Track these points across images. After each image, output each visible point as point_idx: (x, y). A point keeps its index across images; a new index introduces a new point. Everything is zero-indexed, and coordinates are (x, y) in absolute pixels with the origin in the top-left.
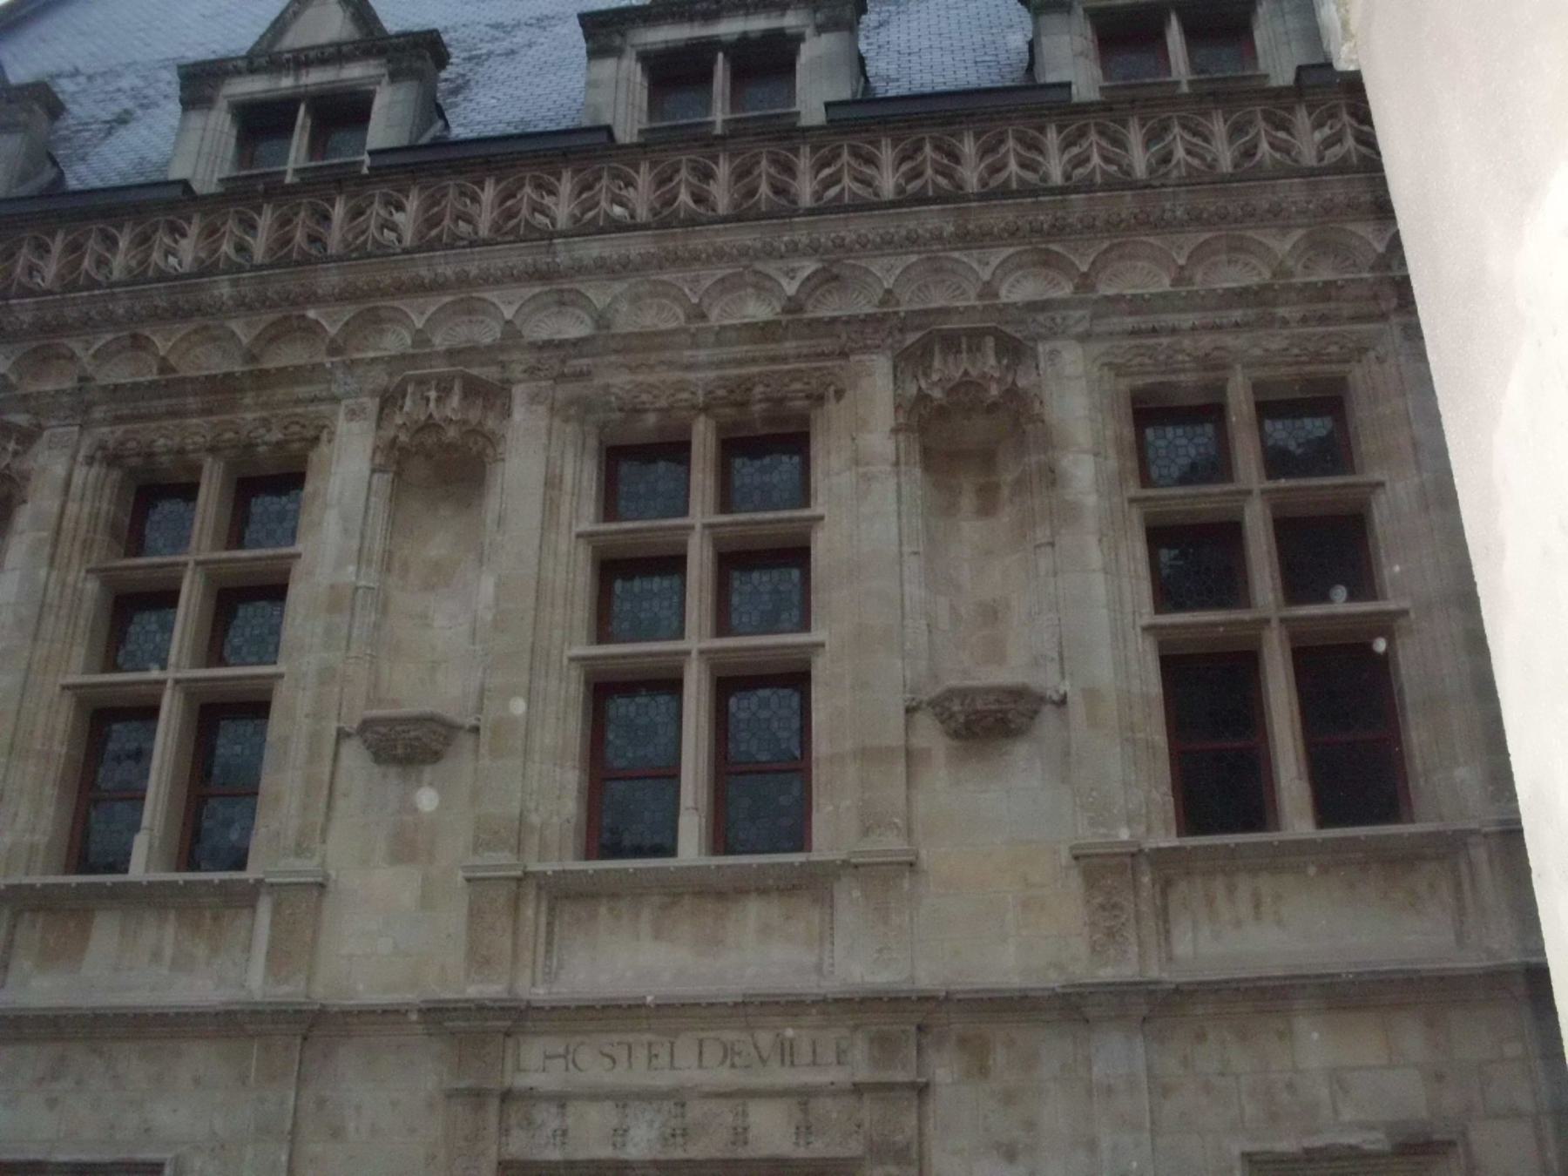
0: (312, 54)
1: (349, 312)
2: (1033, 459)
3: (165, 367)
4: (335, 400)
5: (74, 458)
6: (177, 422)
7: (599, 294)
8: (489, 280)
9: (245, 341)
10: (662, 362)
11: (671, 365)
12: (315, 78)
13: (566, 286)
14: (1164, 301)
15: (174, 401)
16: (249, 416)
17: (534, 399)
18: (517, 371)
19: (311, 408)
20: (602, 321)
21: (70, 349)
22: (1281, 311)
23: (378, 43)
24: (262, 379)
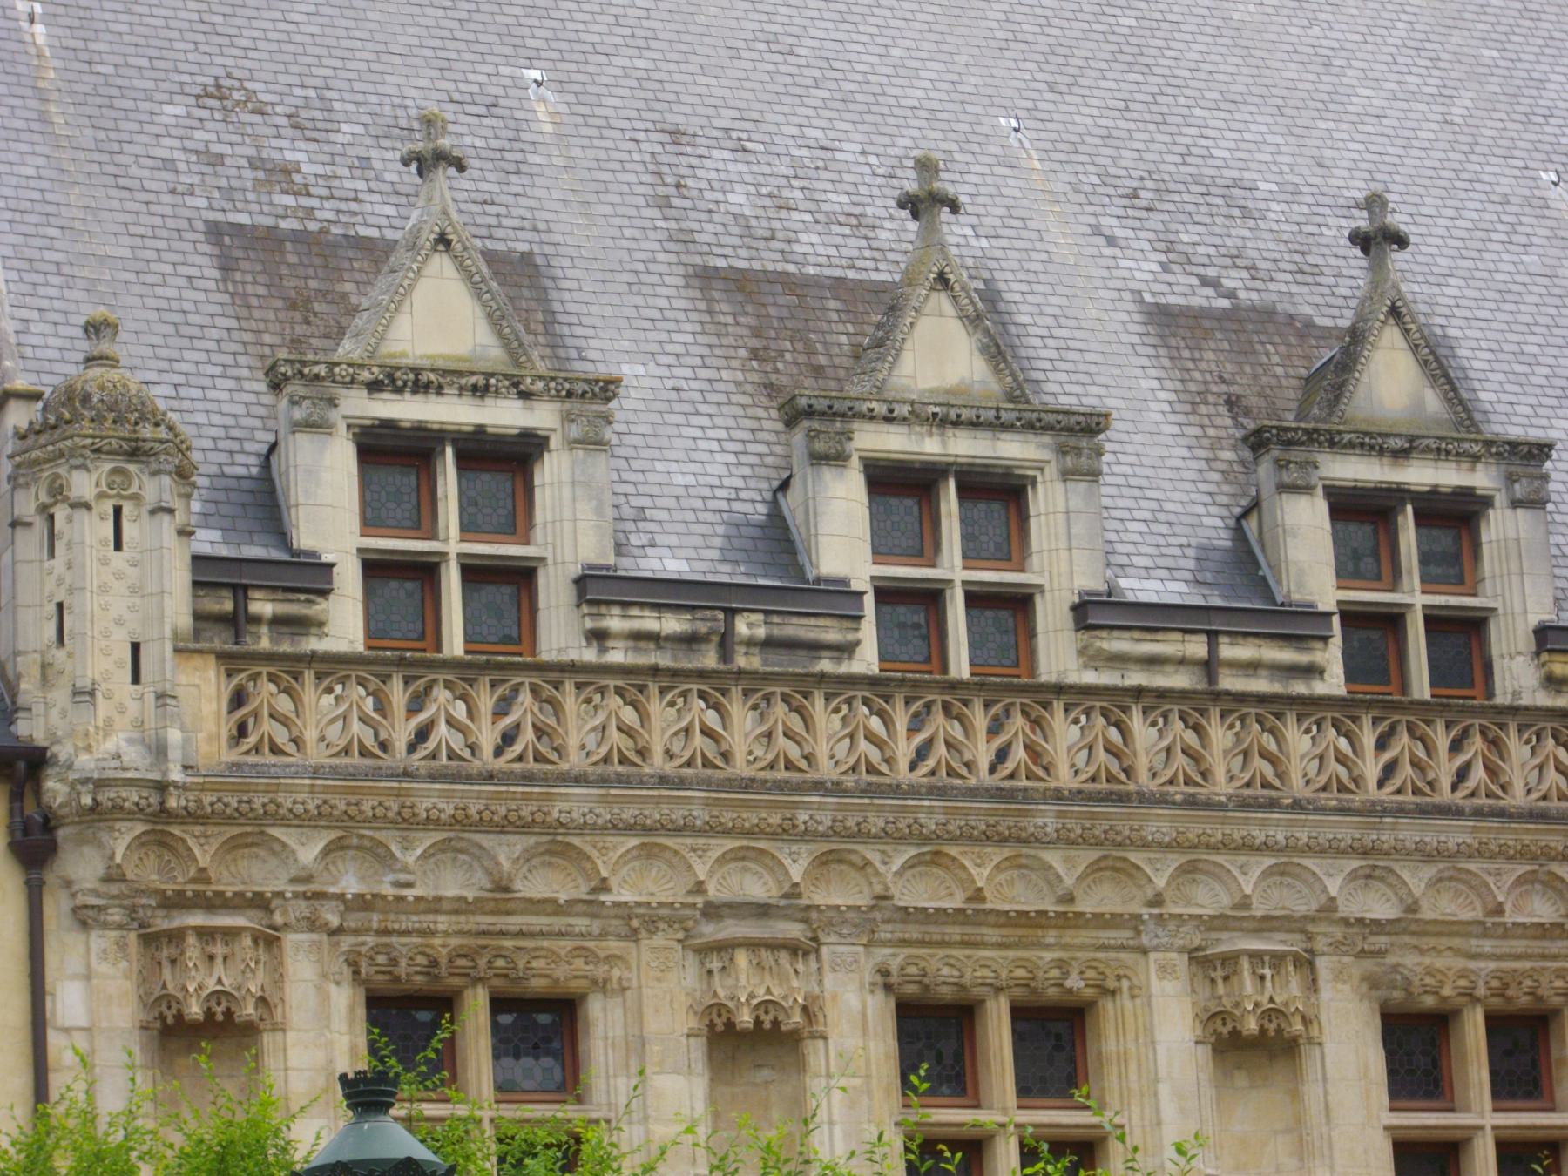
0: (966, 414)
1: (1175, 860)
3: (978, 895)
4: (1144, 952)
5: (862, 986)
6: (968, 952)
7: (1416, 878)
8: (1310, 849)
10: (1450, 948)
11: (1457, 952)
12: (964, 446)
13: (1381, 863)
15: (969, 929)
16: (1048, 956)
17: (1338, 976)
18: (1320, 944)
19: (1112, 955)
20: (1413, 908)
21: (864, 858)
23: (1043, 415)
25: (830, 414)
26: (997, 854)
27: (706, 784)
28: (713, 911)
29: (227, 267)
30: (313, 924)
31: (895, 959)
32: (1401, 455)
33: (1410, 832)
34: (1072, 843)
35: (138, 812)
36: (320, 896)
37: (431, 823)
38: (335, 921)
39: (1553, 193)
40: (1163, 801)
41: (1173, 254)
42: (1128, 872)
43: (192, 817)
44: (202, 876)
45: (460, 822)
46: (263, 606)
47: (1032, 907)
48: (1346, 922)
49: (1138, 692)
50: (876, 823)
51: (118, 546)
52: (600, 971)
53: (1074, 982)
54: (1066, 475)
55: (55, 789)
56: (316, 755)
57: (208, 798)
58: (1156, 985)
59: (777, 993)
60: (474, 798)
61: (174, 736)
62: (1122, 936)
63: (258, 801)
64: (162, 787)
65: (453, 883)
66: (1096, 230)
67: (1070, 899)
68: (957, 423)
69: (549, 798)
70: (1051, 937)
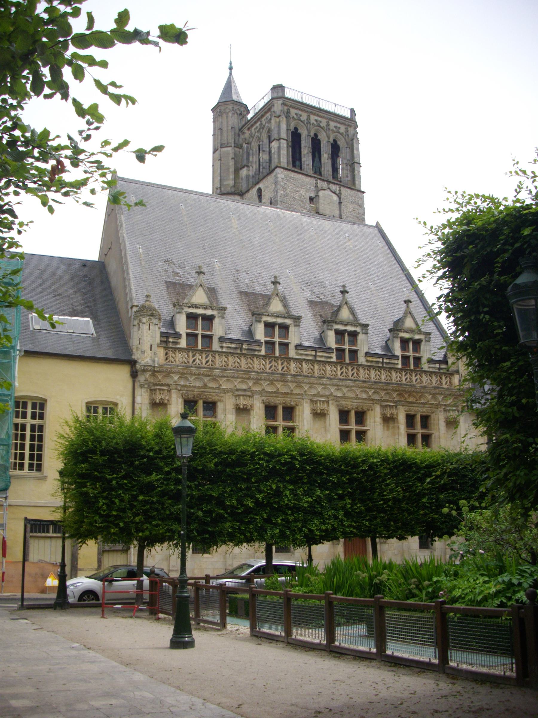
1: (308, 385)
2: (396, 424)
3: (278, 390)
4: (303, 399)
7: (345, 390)
8: (329, 385)
9: (292, 388)
12: (279, 320)
14: (414, 403)
17: (332, 404)
18: (330, 399)
20: (344, 394)
22: (426, 406)
24: (293, 394)
25: (259, 314)
26: (282, 383)
27: (237, 370)
28: (237, 390)
29: (168, 288)
30: (176, 389)
31: (265, 399)
32: (346, 325)
33: (345, 383)
34: (293, 382)
35: (150, 371)
36: (178, 385)
37: (195, 374)
38: (179, 388)
39: (371, 286)
40: (307, 376)
41: (313, 293)
42: (301, 387)
43: (159, 372)
44: (160, 381)
45: (199, 374)
46: (171, 340)
47: (286, 391)
48: (334, 396)
49: (304, 360)
50: (263, 378)
51: (149, 329)
52: (220, 398)
53: (292, 403)
54: (295, 325)
55: (138, 366)
56: (178, 363)
57: (161, 369)
58: (305, 404)
59: (247, 403)
60: (202, 371)
61: (156, 359)
62: (300, 397)
63: (169, 370)
64: (154, 367)
65: (198, 384)
66: (301, 288)
67: (292, 391)
68: (278, 317)
69: (213, 371)
70: (289, 396)
